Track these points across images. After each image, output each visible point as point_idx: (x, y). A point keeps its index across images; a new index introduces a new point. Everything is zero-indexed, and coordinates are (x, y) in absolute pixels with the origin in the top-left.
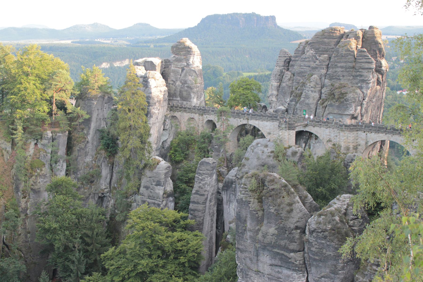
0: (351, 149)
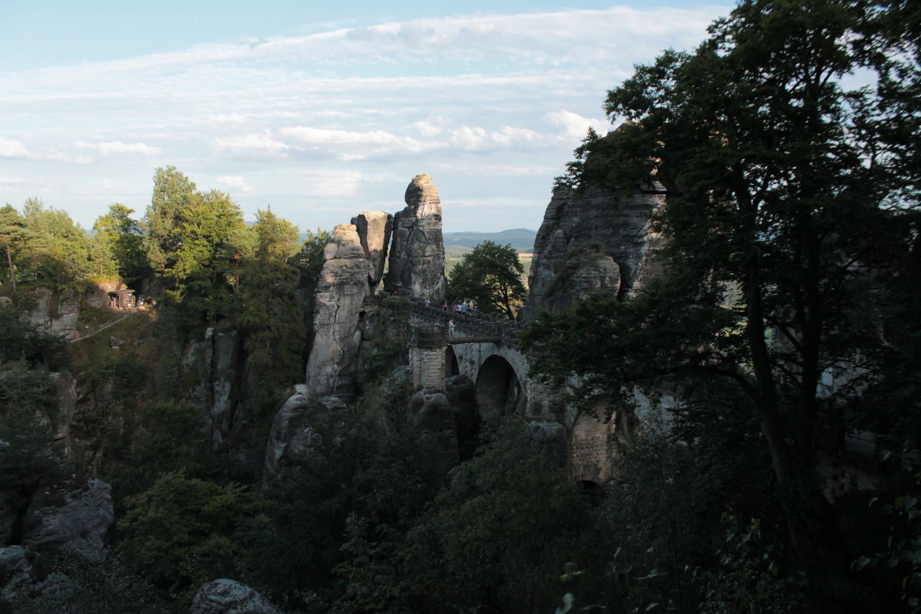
0: (546, 410)
